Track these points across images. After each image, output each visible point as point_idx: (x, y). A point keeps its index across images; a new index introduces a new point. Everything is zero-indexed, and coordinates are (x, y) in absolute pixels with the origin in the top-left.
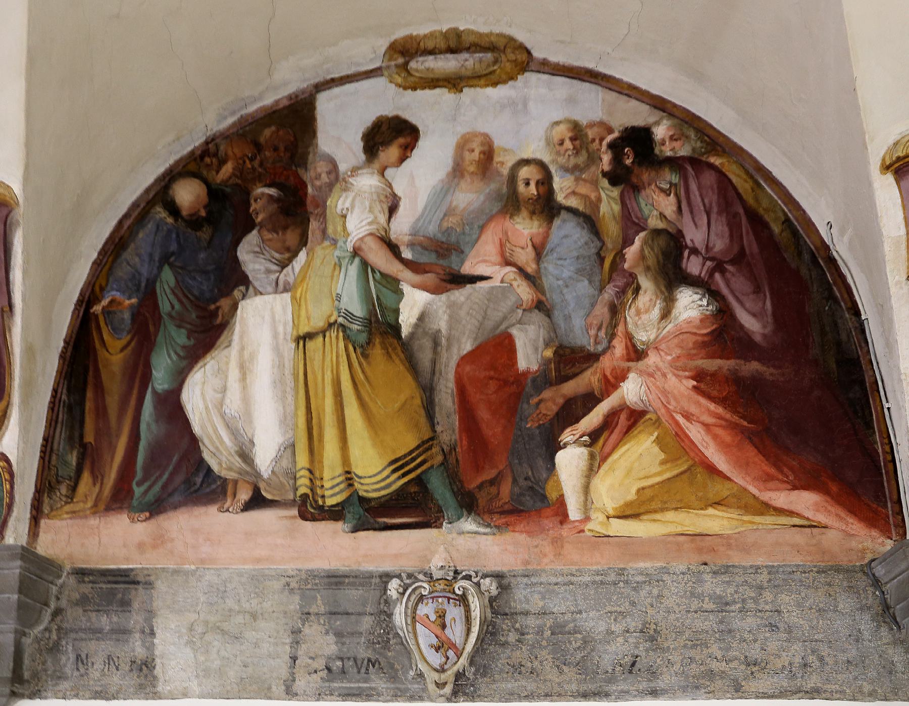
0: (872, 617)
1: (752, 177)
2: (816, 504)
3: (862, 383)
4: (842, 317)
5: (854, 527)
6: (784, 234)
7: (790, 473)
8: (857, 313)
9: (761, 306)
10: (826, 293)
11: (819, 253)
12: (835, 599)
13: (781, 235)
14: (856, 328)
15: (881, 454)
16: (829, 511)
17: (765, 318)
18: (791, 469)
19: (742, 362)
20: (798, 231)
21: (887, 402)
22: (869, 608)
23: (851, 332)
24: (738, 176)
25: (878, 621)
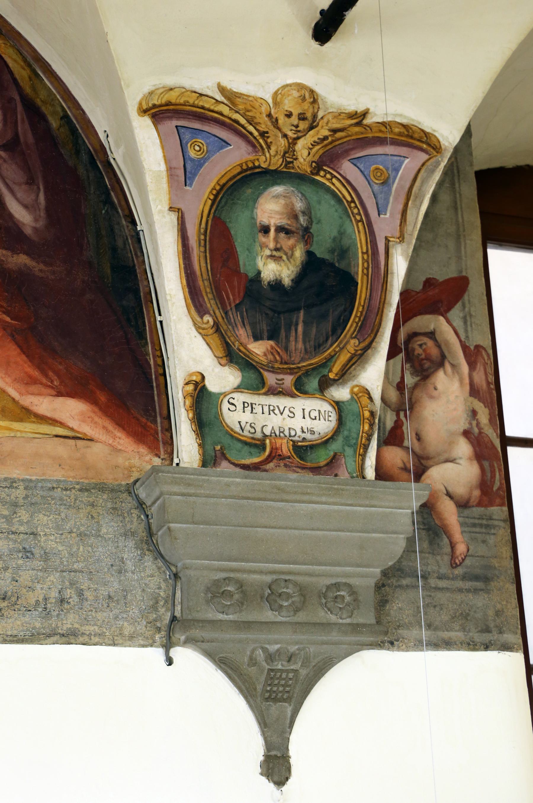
0: (136, 544)
1: (29, 65)
2: (82, 414)
3: (136, 292)
4: (119, 223)
5: (122, 441)
6: (62, 130)
7: (56, 377)
8: (134, 223)
9: (34, 198)
10: (103, 196)
11: (97, 156)
12: (98, 522)
13: (58, 129)
14: (132, 236)
15: (152, 366)
16: (96, 423)
17: (38, 212)
18: (57, 373)
19: (9, 253)
20: (77, 130)
21: (160, 315)
22: (133, 534)
23: (127, 239)
24: (15, 61)
25: (142, 549)
